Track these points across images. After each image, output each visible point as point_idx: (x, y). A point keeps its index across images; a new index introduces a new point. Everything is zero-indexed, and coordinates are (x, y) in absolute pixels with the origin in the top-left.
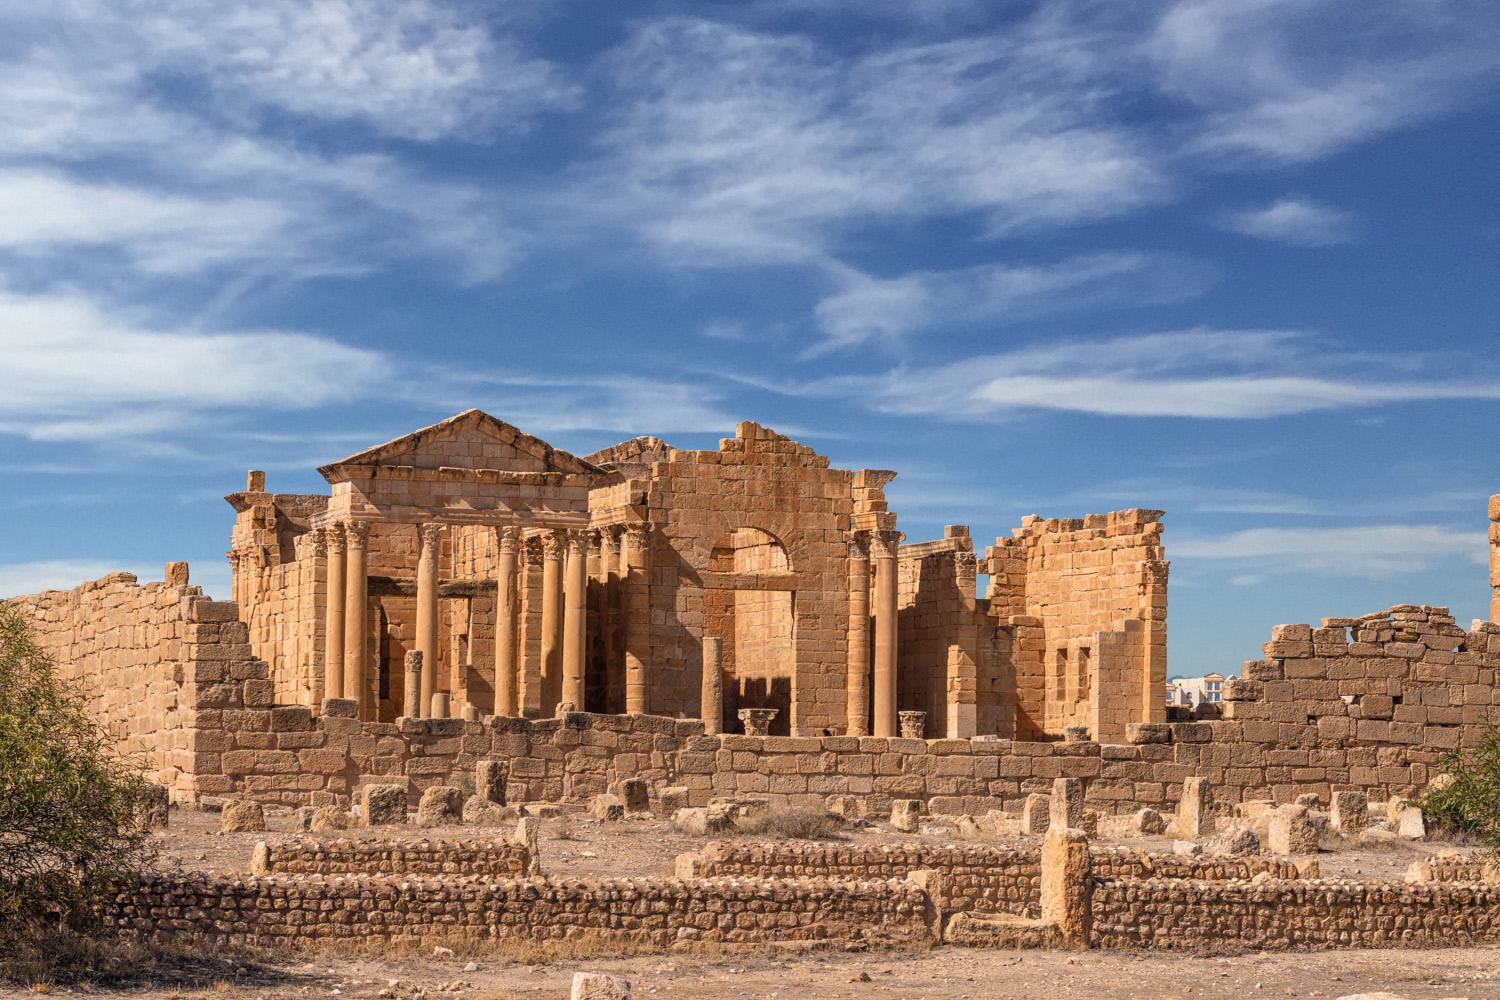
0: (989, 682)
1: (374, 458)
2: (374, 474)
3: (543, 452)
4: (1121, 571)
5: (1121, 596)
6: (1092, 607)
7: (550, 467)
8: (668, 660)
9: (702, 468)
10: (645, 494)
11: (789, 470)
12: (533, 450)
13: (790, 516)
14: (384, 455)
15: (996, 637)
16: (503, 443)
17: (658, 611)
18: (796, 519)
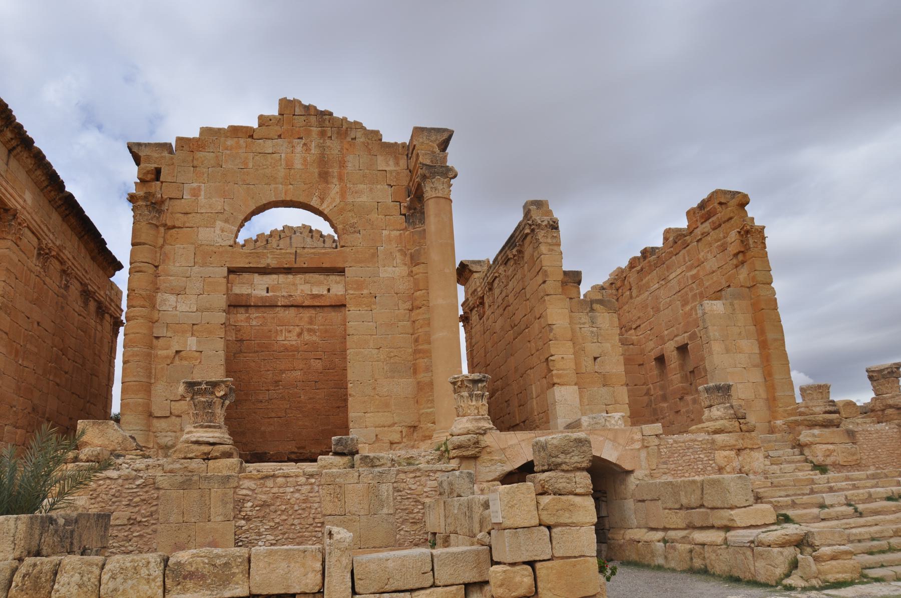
0: (591, 361)
4: (709, 256)
5: (715, 279)
6: (683, 306)
9: (230, 142)
10: (158, 172)
11: (334, 147)
13: (335, 189)
15: (592, 310)
17: (166, 296)
18: (343, 193)
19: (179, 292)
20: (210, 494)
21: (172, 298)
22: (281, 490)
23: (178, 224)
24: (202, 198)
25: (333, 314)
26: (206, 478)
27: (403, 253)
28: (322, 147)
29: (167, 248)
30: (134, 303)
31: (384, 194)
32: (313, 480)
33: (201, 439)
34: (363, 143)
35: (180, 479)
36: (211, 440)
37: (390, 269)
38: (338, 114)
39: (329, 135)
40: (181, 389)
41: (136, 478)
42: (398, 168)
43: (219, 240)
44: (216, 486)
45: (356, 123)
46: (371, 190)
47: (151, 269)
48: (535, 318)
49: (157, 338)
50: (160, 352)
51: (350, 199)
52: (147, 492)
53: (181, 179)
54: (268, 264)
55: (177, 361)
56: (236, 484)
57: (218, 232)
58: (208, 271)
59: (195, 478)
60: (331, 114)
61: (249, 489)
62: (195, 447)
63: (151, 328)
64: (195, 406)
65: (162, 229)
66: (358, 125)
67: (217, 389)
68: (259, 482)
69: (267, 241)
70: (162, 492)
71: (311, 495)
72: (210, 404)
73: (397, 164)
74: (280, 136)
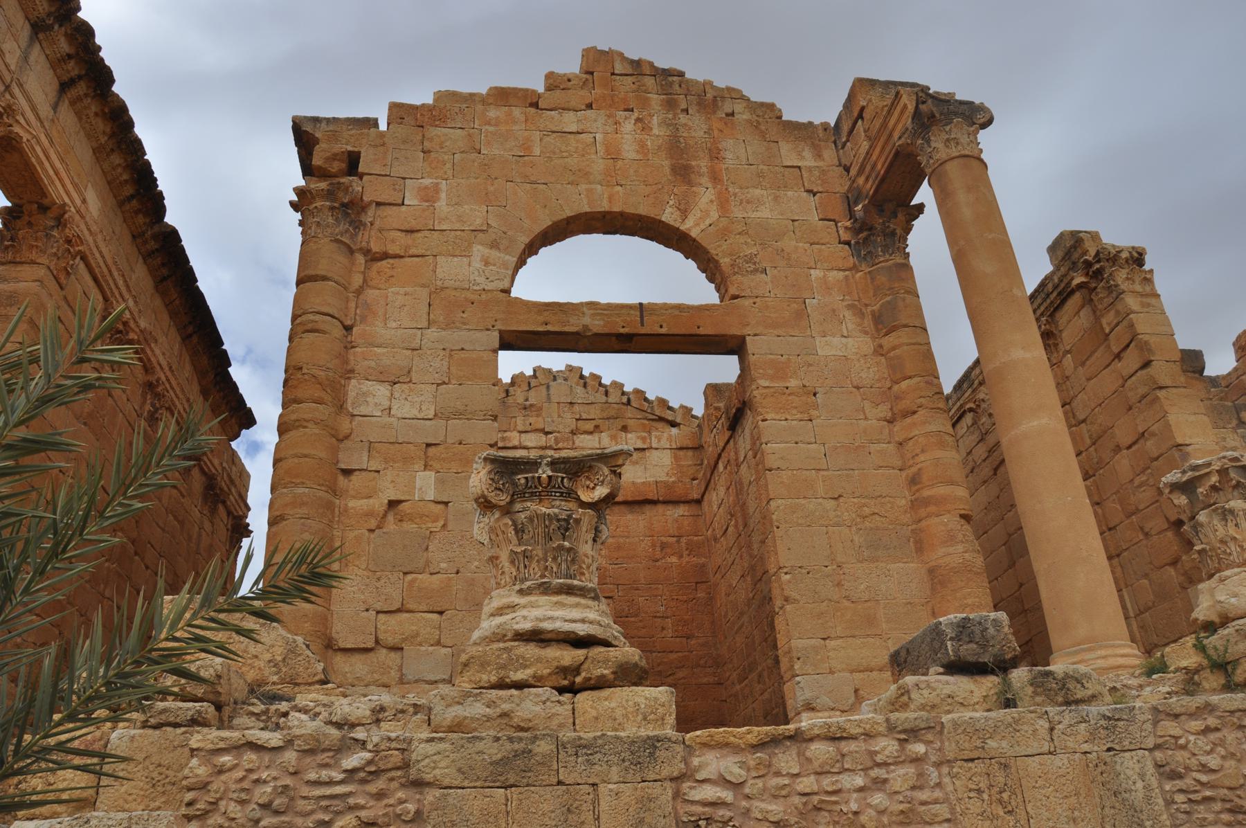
9: (493, 113)
11: (696, 126)
13: (706, 196)
17: (368, 386)
18: (723, 203)
20: (596, 802)
21: (382, 391)
22: (827, 783)
23: (393, 249)
24: (442, 204)
25: (630, 517)
26: (580, 746)
29: (371, 294)
30: (299, 394)
32: (920, 748)
33: (547, 626)
34: (749, 121)
35: (495, 752)
36: (582, 629)
37: (836, 340)
38: (694, 73)
39: (684, 106)
40: (479, 479)
41: (342, 748)
42: (821, 164)
43: (481, 280)
44: (615, 773)
45: (729, 89)
46: (776, 198)
47: (338, 331)
48: (1118, 449)
49: (347, 472)
50: (352, 504)
51: (738, 213)
52: (380, 796)
53: (398, 170)
54: (585, 327)
55: (391, 525)
56: (678, 768)
57: (477, 264)
58: (456, 337)
59: (543, 747)
60: (681, 74)
61: (723, 782)
62: (530, 650)
63: (335, 451)
64: (519, 531)
65: (360, 259)
66: (734, 94)
67: (583, 480)
68: (752, 759)
69: (507, 391)
70: (431, 795)
71: (924, 795)
72: (566, 526)
73: (819, 156)
74: (590, 106)
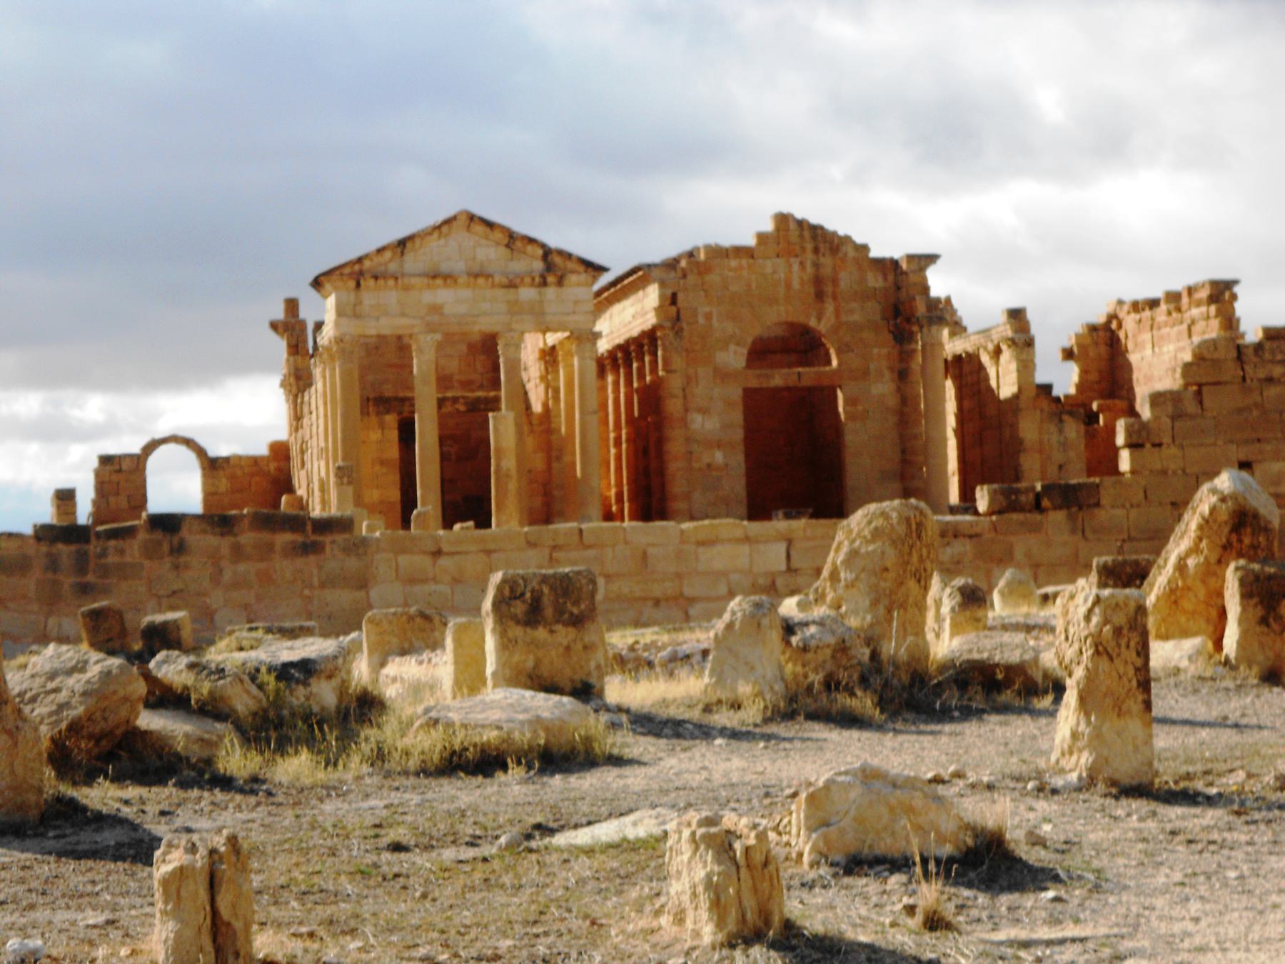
1: (357, 267)
2: (358, 285)
3: (540, 252)
7: (550, 267)
8: (709, 466)
9: (734, 263)
11: (827, 261)
12: (529, 248)
13: (830, 308)
14: (367, 264)
15: (1061, 421)
16: (498, 244)
18: (837, 312)
19: (704, 411)
24: (715, 322)
27: (891, 369)
28: (816, 265)
31: (873, 310)
51: (844, 318)
60: (822, 228)
66: (847, 239)
73: (885, 279)
